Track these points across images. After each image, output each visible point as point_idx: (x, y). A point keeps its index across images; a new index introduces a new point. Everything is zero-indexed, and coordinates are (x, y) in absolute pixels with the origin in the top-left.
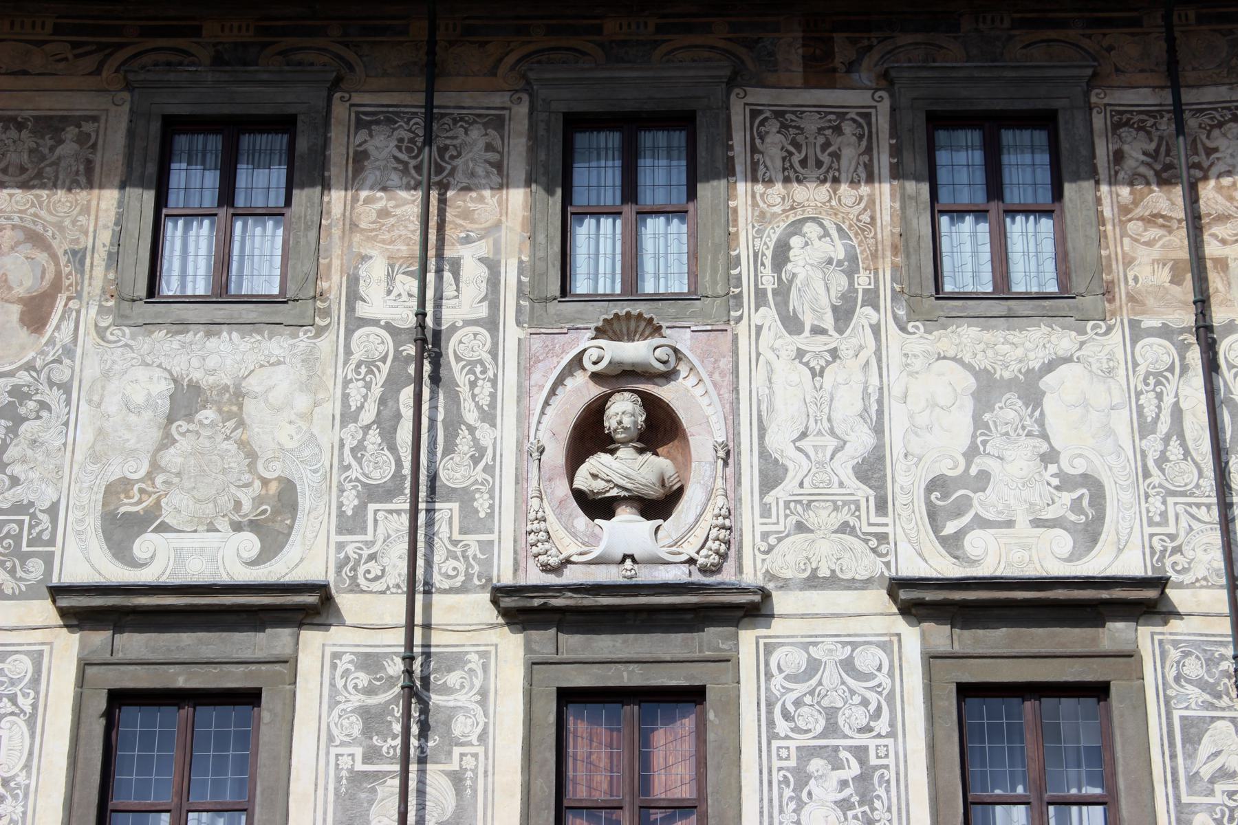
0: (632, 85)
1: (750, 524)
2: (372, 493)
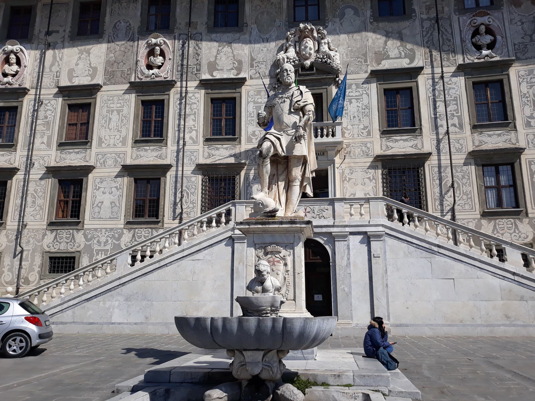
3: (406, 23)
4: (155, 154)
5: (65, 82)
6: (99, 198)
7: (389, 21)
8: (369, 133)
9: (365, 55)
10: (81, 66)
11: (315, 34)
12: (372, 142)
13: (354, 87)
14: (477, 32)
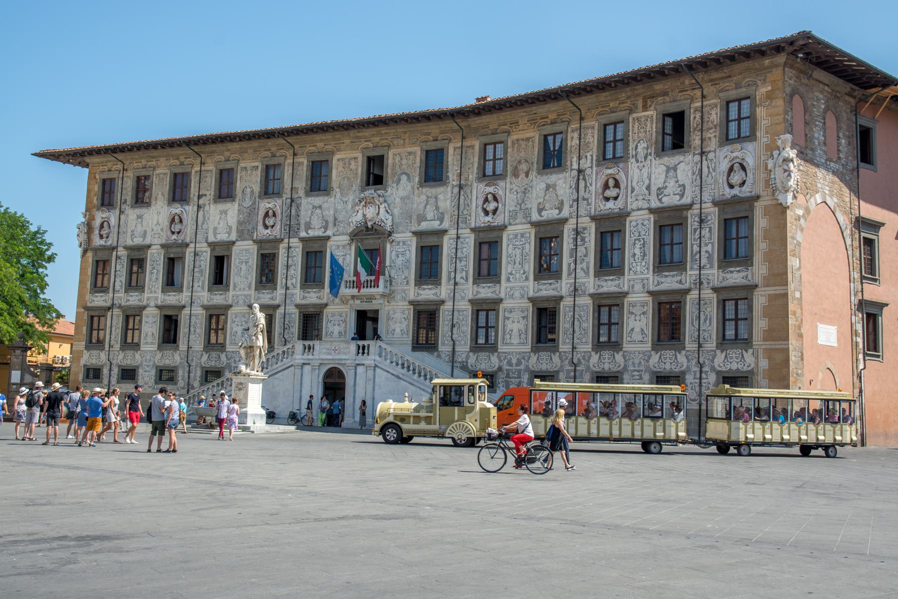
0: (614, 117)
1: (629, 200)
2: (574, 201)
3: (441, 189)
4: (269, 296)
5: (211, 239)
6: (235, 329)
7: (431, 187)
8: (407, 283)
9: (411, 217)
10: (221, 225)
12: (409, 290)
13: (401, 244)
14: (486, 200)
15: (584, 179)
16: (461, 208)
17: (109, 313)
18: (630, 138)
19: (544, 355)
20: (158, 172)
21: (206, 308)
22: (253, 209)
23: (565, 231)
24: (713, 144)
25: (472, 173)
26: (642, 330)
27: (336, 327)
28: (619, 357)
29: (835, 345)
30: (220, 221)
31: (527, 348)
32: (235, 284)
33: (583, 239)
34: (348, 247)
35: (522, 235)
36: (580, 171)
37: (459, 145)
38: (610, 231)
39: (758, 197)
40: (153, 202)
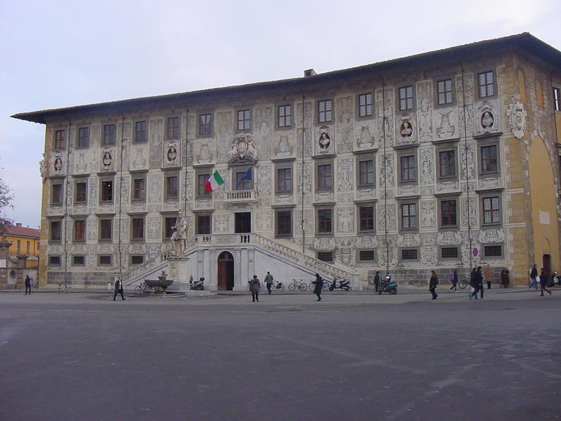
3: (289, 132)
5: (132, 169)
9: (270, 150)
11: (246, 140)
15: (388, 123)
16: (305, 143)
17: (64, 220)
18: (417, 96)
19: (366, 238)
20: (93, 125)
21: (130, 215)
22: (160, 147)
23: (377, 157)
24: (470, 101)
25: (311, 120)
26: (431, 219)
27: (222, 224)
28: (417, 237)
29: (549, 224)
30: (137, 156)
31: (355, 234)
32: (149, 198)
33: (389, 162)
34: (227, 171)
35: (347, 160)
36: (384, 118)
37: (301, 102)
38: (407, 154)
39: (501, 134)
40: (91, 145)
